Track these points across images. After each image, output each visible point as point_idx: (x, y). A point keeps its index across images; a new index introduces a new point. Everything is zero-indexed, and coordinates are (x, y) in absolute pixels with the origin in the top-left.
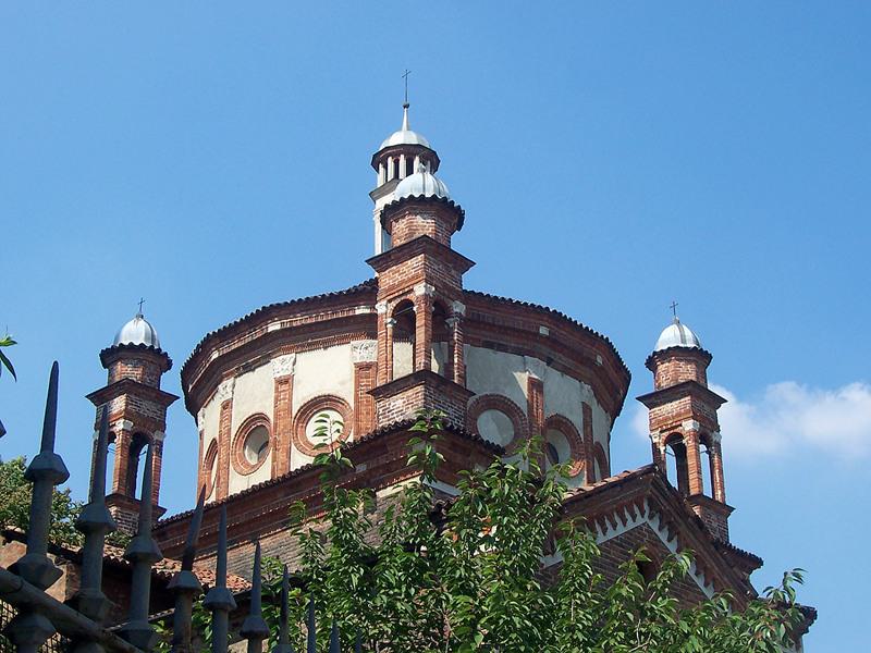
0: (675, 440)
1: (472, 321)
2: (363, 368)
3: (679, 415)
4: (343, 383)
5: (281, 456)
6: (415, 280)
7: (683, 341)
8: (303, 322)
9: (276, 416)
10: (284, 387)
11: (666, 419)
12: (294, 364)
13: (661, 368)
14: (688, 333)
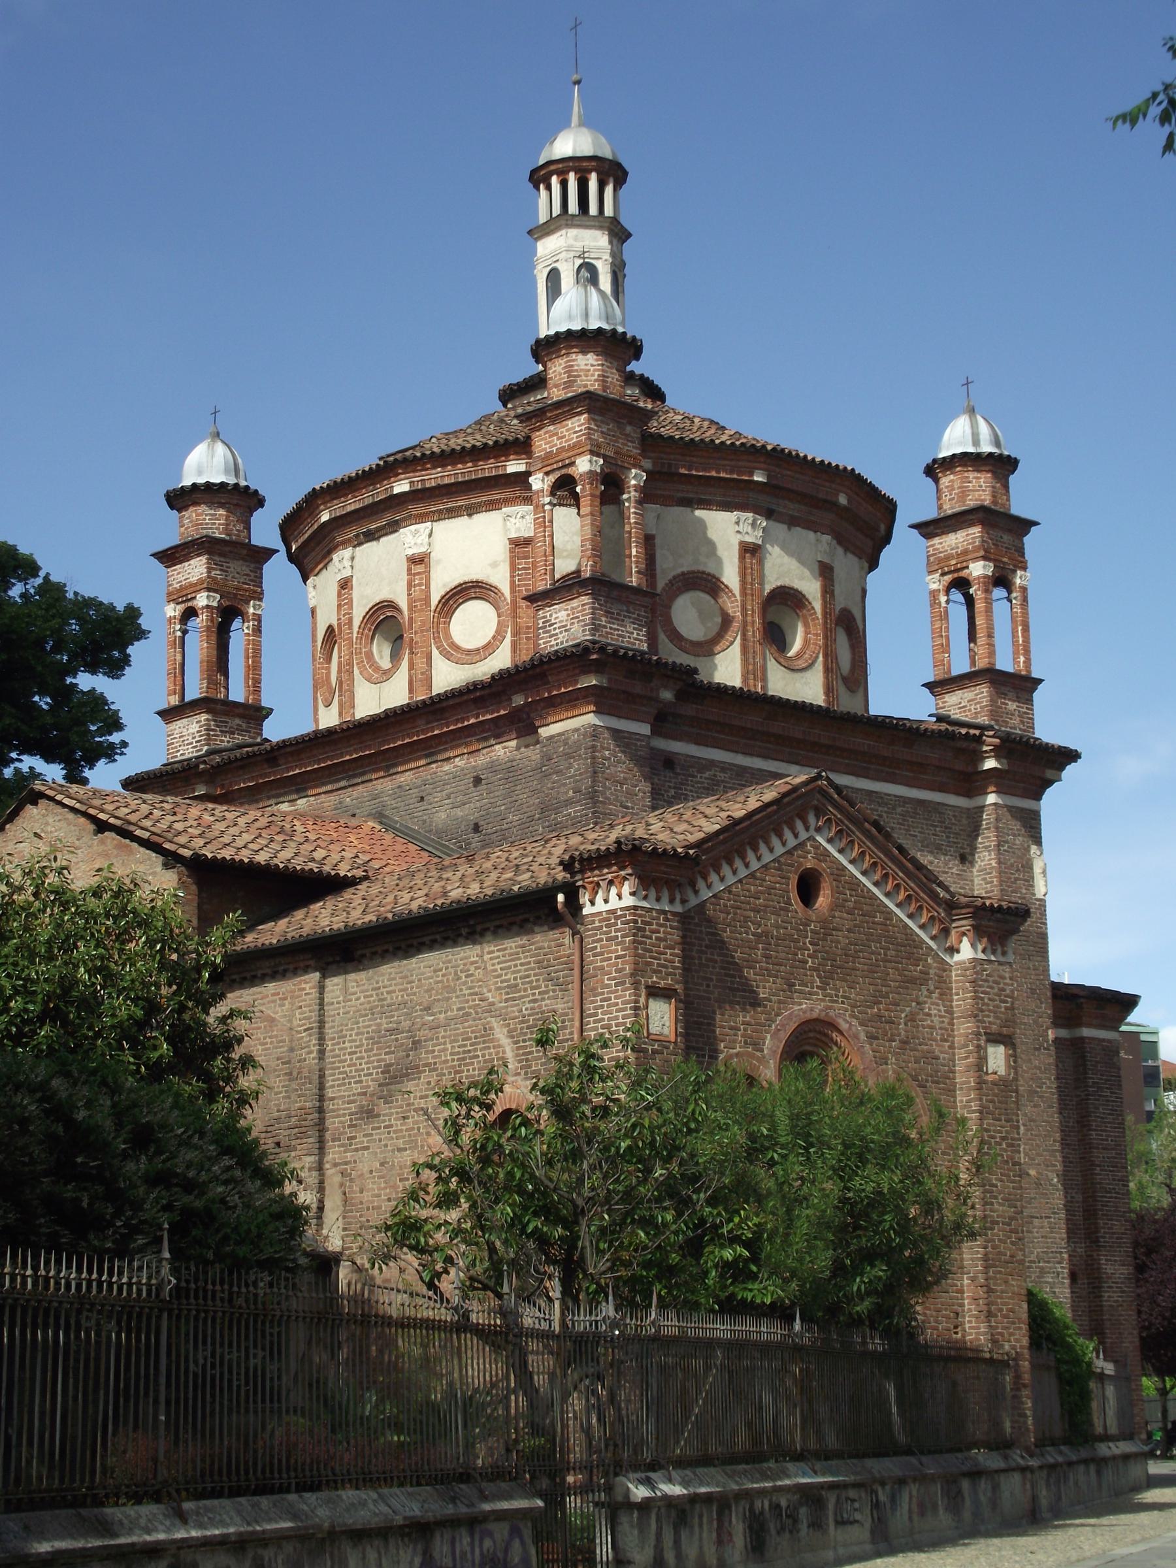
0: (961, 584)
1: (659, 473)
2: (519, 545)
3: (965, 552)
4: (494, 565)
5: (420, 662)
6: (576, 450)
7: (976, 442)
8: (439, 481)
9: (411, 608)
10: (419, 568)
11: (949, 557)
12: (430, 536)
13: (945, 481)
14: (984, 429)
